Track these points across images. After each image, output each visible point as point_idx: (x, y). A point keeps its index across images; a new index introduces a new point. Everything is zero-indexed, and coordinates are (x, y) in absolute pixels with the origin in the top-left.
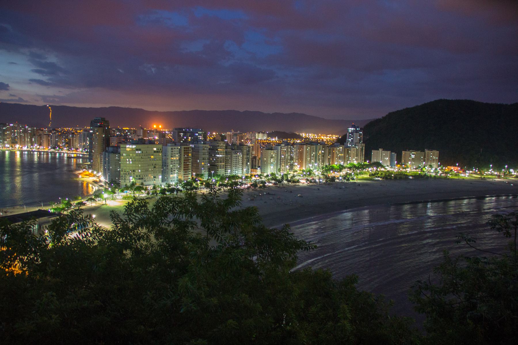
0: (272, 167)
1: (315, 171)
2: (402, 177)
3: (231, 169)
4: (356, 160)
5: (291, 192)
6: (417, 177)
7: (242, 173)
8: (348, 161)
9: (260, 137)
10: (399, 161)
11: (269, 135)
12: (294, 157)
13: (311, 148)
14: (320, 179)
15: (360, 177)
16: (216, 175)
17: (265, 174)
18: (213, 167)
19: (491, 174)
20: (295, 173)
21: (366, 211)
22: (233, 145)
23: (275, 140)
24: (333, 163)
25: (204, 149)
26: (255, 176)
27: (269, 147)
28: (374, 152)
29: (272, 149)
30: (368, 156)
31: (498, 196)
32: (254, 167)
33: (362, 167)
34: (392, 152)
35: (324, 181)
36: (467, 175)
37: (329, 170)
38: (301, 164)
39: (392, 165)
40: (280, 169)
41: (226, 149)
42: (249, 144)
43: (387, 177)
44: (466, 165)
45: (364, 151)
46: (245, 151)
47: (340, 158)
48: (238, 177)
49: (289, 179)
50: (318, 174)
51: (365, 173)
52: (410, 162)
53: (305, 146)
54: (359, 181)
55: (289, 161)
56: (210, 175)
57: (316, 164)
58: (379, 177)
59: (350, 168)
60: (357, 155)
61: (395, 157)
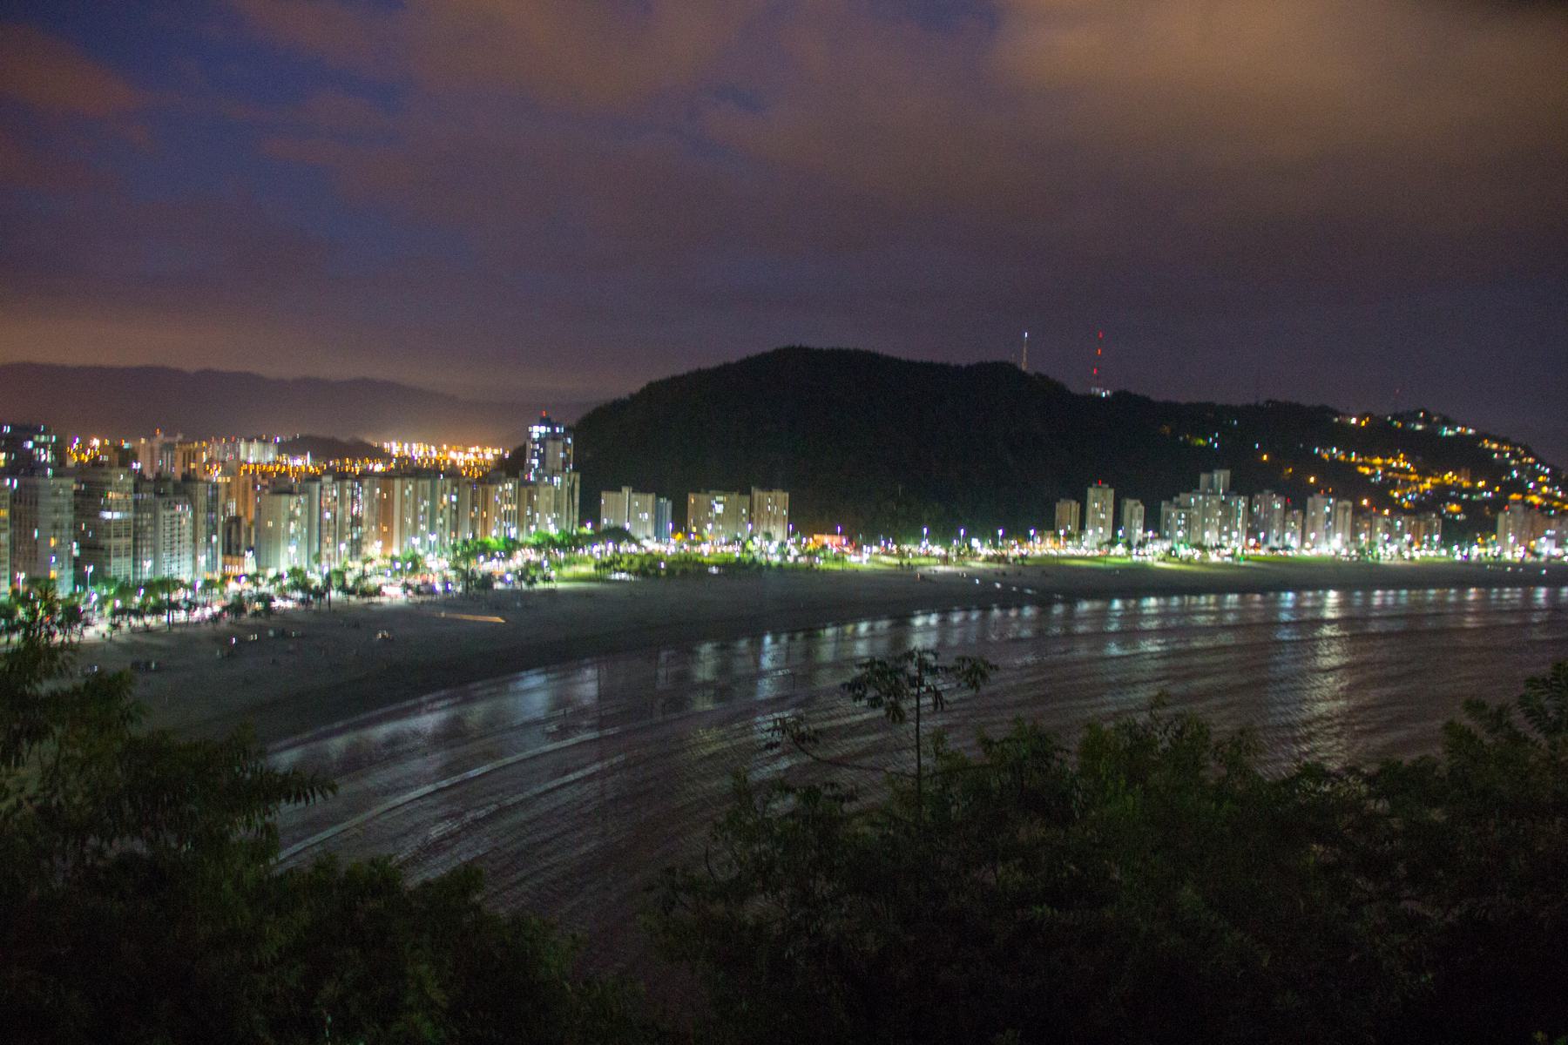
0: (293, 549)
1: (430, 556)
2: (688, 569)
3: (156, 559)
4: (555, 521)
5: (357, 626)
6: (732, 569)
7: (195, 569)
8: (531, 523)
9: (254, 454)
10: (680, 524)
11: (282, 448)
12: (365, 517)
13: (416, 488)
14: (446, 582)
15: (568, 572)
16: (100, 577)
17: (271, 573)
18: (94, 550)
19: (929, 555)
20: (369, 568)
21: (590, 673)
22: (160, 479)
23: (302, 463)
24: (486, 532)
25: (56, 494)
26: (237, 579)
27: (280, 485)
28: (606, 499)
29: (290, 492)
30: (590, 511)
31: (945, 612)
32: (232, 550)
33: (572, 543)
34: (658, 496)
35: (459, 589)
36: (867, 559)
37: (475, 554)
38: (387, 539)
39: (659, 535)
40: (319, 554)
41: (136, 491)
42: (217, 475)
43: (648, 568)
44: (862, 531)
45: (577, 494)
46: (202, 500)
47: (507, 516)
48: (179, 584)
49: (350, 584)
50: (438, 567)
51: (583, 561)
52: (709, 526)
53: (397, 483)
54: (560, 586)
55: (348, 529)
56: (80, 579)
57: (433, 538)
58: (622, 571)
59: (538, 547)
60: (557, 508)
61: (669, 512)
